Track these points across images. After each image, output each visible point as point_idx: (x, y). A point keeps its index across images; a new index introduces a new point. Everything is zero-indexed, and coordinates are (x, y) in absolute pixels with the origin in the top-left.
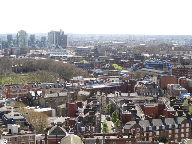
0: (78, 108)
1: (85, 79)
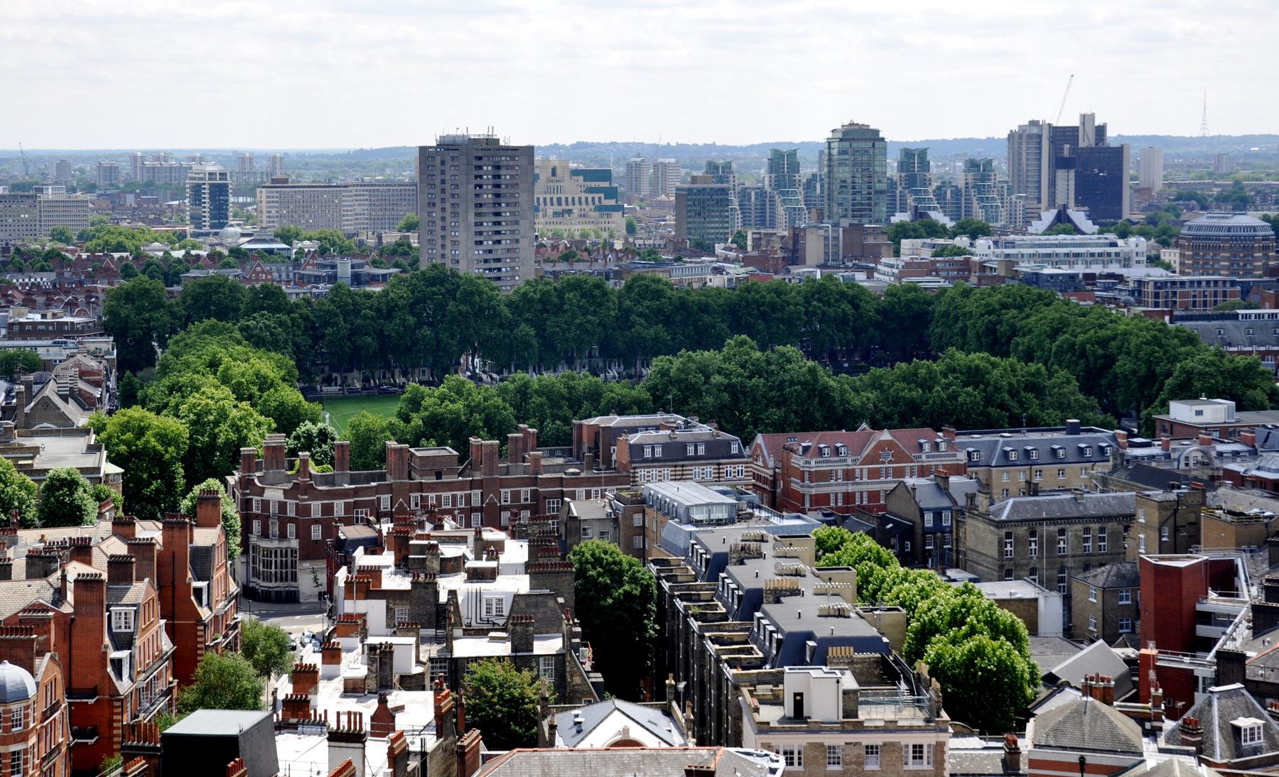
0: (1213, 595)
1: (1250, 417)
